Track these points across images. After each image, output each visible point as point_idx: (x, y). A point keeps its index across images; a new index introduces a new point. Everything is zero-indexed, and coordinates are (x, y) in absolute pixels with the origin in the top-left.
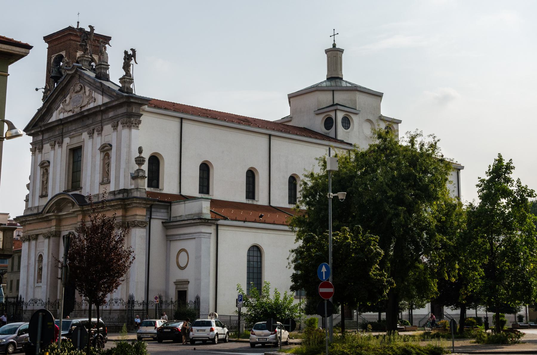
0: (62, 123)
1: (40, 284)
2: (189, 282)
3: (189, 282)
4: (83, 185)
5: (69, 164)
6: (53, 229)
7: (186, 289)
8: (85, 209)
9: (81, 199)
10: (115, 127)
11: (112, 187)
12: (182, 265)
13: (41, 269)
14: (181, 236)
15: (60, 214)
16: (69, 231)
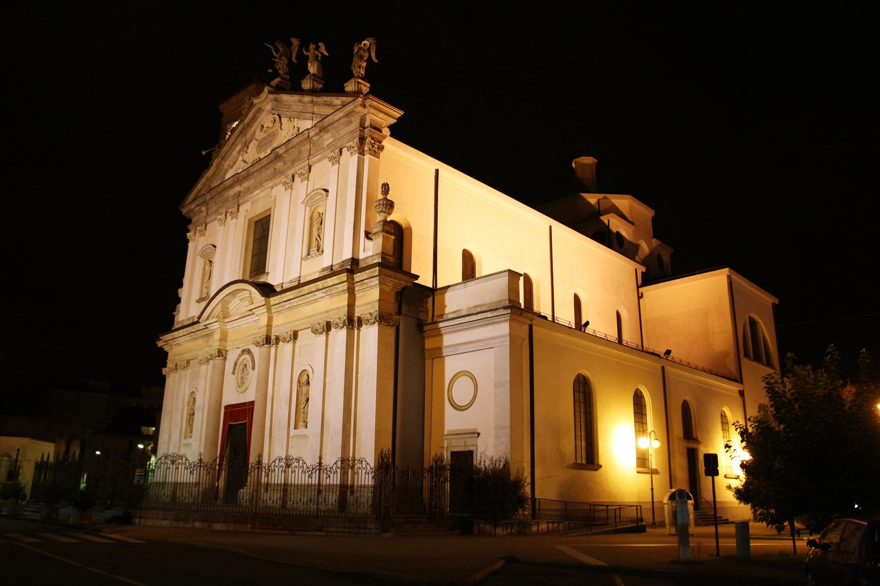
0: (238, 179)
1: (189, 441)
2: (479, 434)
3: (479, 434)
4: (269, 267)
5: (247, 244)
6: (216, 345)
7: (471, 448)
8: (272, 303)
9: (267, 290)
10: (335, 160)
11: (325, 261)
12: (461, 401)
13: (192, 415)
14: (459, 348)
15: (227, 320)
16: (241, 349)
